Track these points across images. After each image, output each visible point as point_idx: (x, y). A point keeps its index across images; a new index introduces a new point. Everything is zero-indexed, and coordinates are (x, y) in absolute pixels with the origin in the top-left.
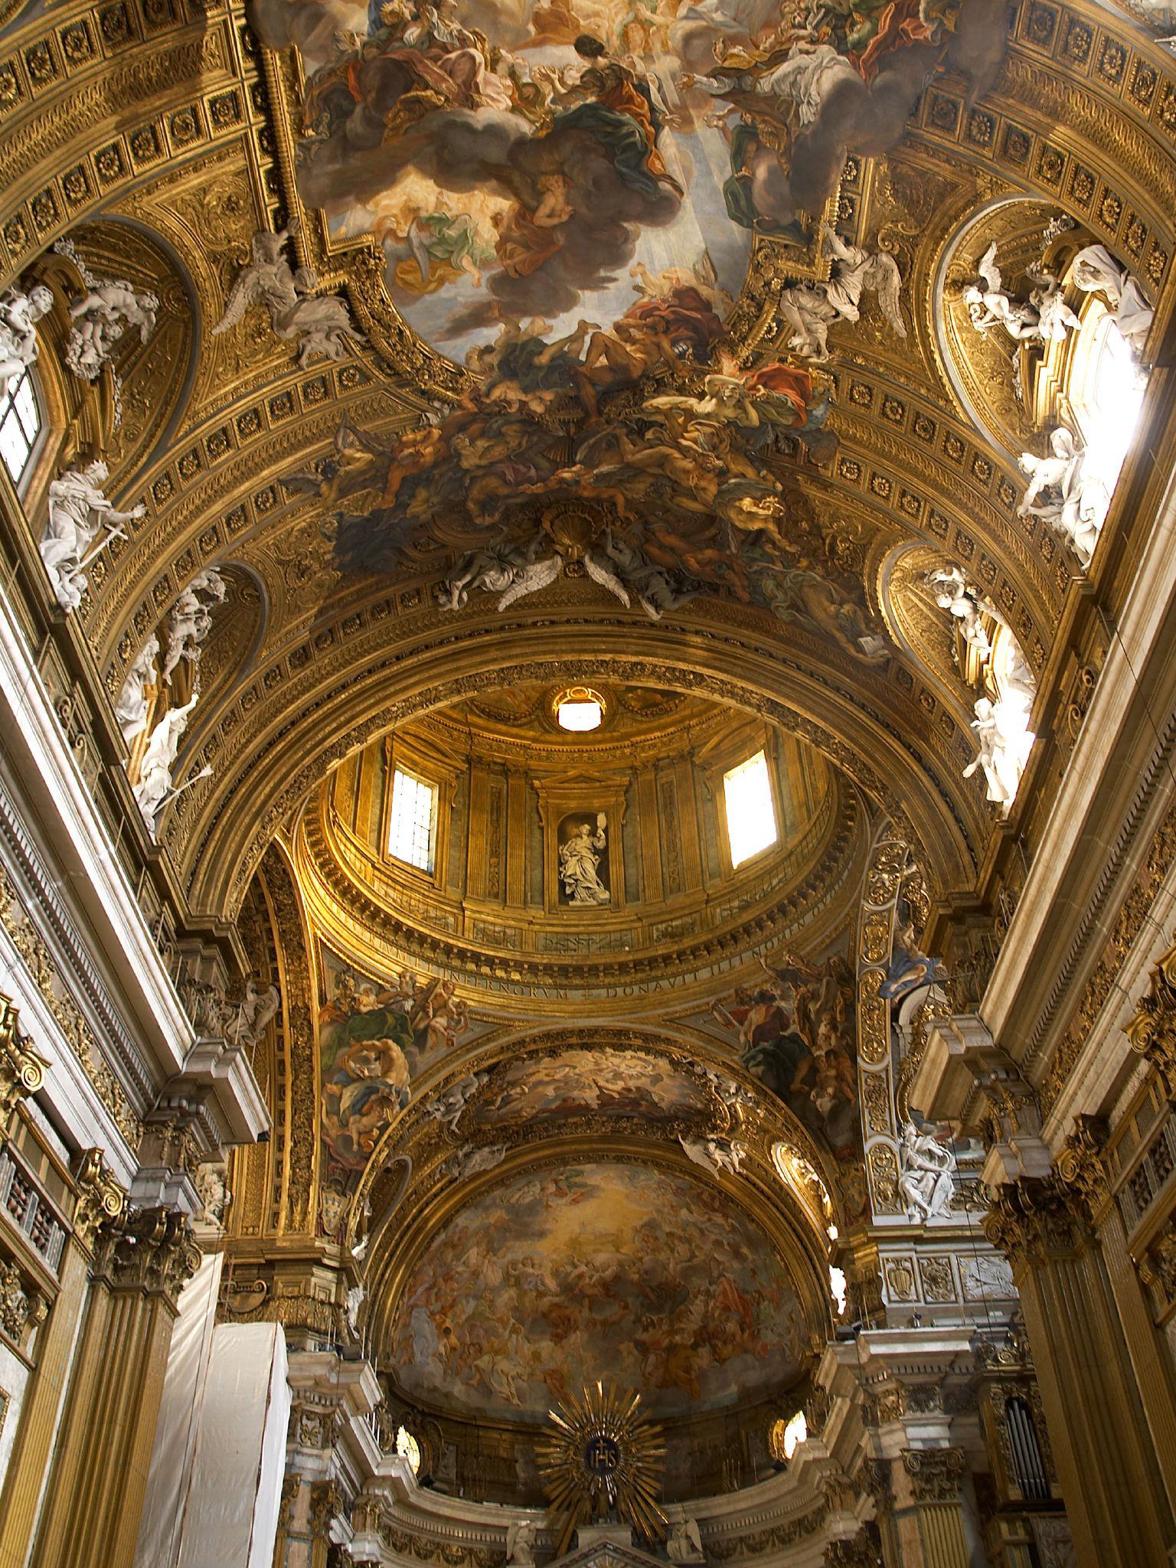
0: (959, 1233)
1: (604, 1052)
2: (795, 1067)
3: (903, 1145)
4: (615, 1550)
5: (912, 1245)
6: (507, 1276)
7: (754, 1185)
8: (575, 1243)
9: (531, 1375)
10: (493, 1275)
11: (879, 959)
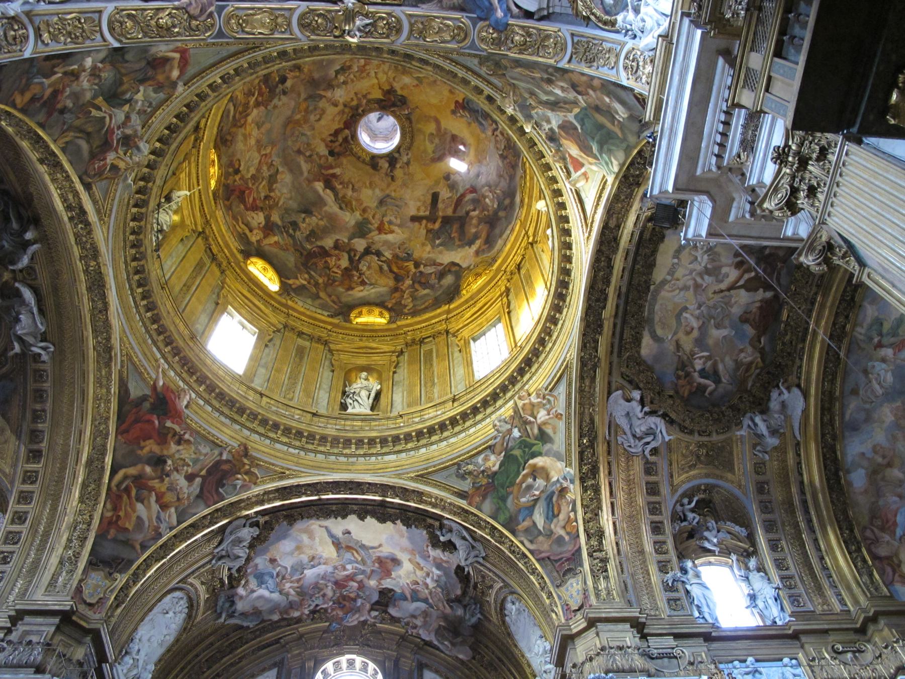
1: (664, 282)
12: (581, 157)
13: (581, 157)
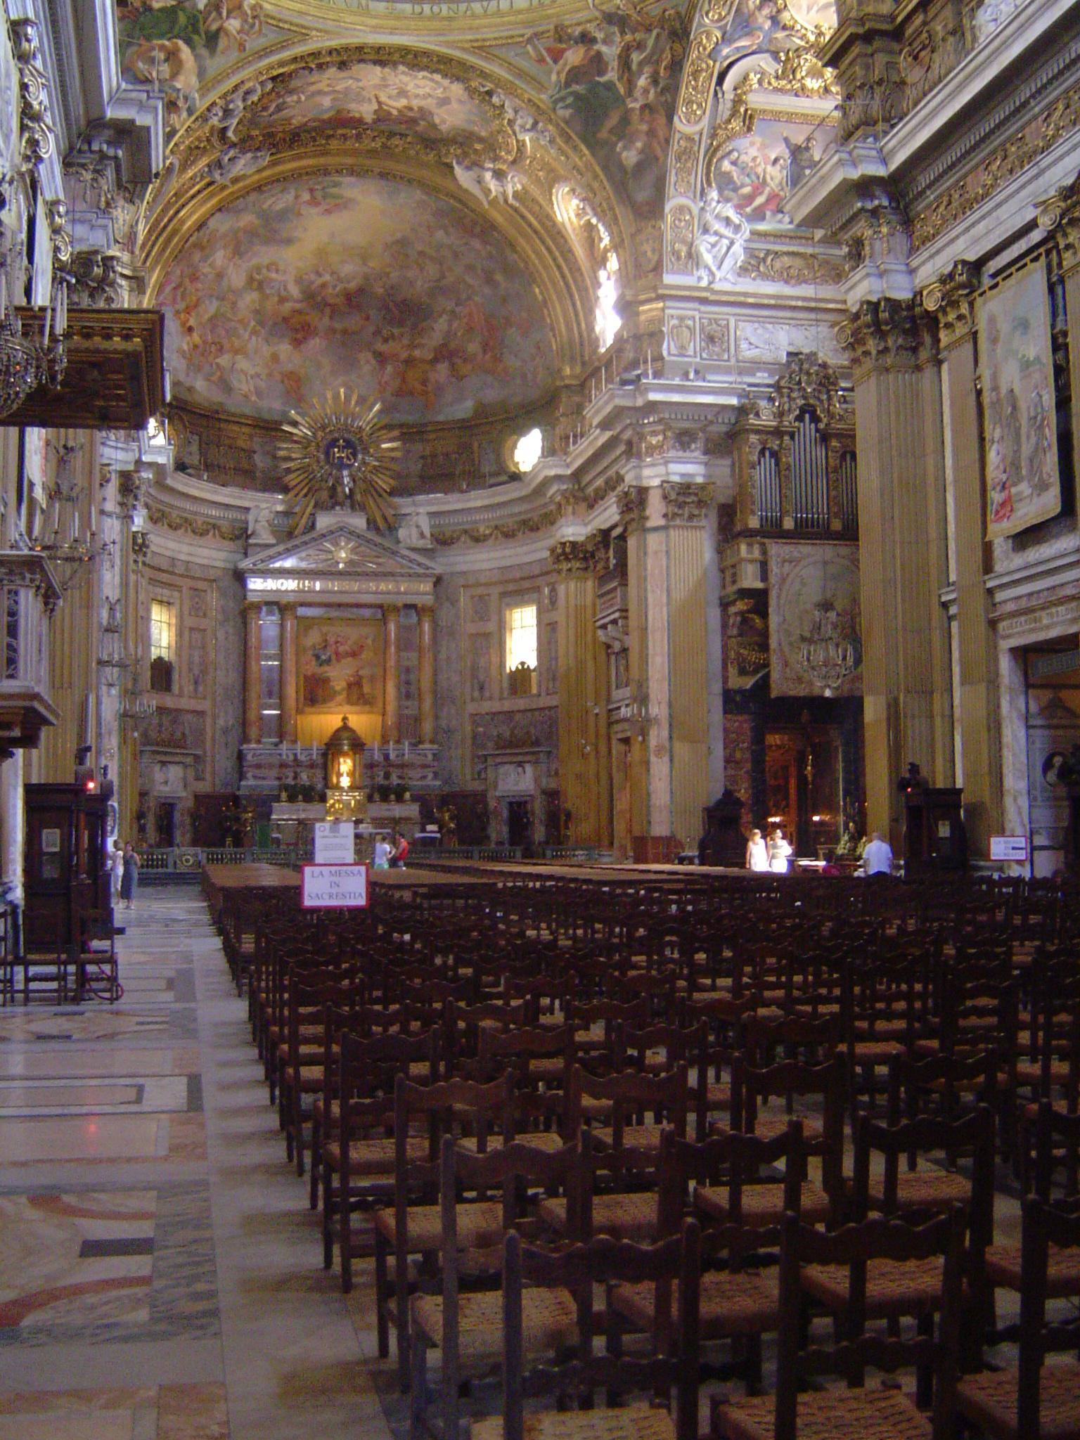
0: (742, 299)
2: (606, 115)
3: (702, 209)
4: (351, 533)
5: (696, 305)
6: (251, 280)
7: (523, 217)
8: (321, 253)
9: (270, 375)
10: (236, 278)
11: (720, 20)
12: (565, 64)
13: (565, 64)
